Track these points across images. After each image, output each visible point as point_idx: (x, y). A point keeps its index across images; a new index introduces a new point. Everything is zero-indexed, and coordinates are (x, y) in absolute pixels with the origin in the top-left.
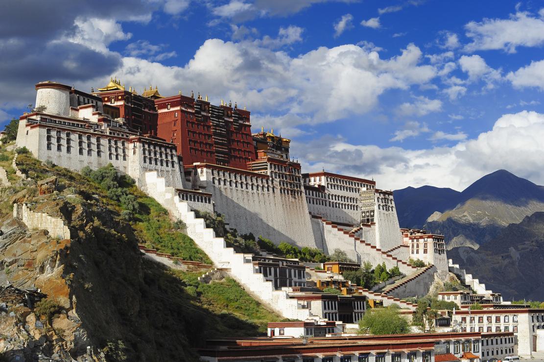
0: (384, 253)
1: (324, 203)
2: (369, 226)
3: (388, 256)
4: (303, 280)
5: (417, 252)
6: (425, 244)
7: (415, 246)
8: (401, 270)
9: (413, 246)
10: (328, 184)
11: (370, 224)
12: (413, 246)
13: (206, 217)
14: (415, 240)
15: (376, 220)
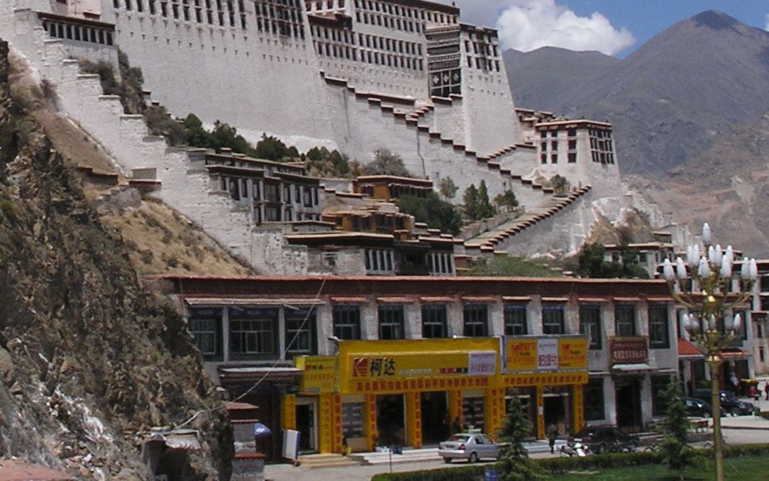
0: (481, 160)
1: (350, 54)
2: (449, 103)
3: (492, 167)
4: (315, 209)
5: (554, 159)
6: (572, 144)
7: (549, 147)
8: (517, 198)
9: (544, 145)
10: (358, 14)
11: (450, 99)
12: (544, 145)
13: (103, 73)
14: (549, 135)
15: (464, 92)
